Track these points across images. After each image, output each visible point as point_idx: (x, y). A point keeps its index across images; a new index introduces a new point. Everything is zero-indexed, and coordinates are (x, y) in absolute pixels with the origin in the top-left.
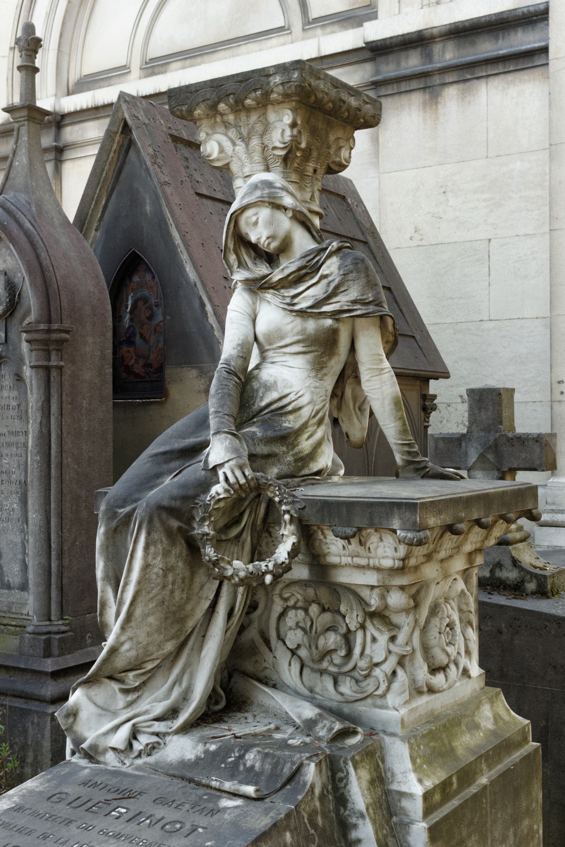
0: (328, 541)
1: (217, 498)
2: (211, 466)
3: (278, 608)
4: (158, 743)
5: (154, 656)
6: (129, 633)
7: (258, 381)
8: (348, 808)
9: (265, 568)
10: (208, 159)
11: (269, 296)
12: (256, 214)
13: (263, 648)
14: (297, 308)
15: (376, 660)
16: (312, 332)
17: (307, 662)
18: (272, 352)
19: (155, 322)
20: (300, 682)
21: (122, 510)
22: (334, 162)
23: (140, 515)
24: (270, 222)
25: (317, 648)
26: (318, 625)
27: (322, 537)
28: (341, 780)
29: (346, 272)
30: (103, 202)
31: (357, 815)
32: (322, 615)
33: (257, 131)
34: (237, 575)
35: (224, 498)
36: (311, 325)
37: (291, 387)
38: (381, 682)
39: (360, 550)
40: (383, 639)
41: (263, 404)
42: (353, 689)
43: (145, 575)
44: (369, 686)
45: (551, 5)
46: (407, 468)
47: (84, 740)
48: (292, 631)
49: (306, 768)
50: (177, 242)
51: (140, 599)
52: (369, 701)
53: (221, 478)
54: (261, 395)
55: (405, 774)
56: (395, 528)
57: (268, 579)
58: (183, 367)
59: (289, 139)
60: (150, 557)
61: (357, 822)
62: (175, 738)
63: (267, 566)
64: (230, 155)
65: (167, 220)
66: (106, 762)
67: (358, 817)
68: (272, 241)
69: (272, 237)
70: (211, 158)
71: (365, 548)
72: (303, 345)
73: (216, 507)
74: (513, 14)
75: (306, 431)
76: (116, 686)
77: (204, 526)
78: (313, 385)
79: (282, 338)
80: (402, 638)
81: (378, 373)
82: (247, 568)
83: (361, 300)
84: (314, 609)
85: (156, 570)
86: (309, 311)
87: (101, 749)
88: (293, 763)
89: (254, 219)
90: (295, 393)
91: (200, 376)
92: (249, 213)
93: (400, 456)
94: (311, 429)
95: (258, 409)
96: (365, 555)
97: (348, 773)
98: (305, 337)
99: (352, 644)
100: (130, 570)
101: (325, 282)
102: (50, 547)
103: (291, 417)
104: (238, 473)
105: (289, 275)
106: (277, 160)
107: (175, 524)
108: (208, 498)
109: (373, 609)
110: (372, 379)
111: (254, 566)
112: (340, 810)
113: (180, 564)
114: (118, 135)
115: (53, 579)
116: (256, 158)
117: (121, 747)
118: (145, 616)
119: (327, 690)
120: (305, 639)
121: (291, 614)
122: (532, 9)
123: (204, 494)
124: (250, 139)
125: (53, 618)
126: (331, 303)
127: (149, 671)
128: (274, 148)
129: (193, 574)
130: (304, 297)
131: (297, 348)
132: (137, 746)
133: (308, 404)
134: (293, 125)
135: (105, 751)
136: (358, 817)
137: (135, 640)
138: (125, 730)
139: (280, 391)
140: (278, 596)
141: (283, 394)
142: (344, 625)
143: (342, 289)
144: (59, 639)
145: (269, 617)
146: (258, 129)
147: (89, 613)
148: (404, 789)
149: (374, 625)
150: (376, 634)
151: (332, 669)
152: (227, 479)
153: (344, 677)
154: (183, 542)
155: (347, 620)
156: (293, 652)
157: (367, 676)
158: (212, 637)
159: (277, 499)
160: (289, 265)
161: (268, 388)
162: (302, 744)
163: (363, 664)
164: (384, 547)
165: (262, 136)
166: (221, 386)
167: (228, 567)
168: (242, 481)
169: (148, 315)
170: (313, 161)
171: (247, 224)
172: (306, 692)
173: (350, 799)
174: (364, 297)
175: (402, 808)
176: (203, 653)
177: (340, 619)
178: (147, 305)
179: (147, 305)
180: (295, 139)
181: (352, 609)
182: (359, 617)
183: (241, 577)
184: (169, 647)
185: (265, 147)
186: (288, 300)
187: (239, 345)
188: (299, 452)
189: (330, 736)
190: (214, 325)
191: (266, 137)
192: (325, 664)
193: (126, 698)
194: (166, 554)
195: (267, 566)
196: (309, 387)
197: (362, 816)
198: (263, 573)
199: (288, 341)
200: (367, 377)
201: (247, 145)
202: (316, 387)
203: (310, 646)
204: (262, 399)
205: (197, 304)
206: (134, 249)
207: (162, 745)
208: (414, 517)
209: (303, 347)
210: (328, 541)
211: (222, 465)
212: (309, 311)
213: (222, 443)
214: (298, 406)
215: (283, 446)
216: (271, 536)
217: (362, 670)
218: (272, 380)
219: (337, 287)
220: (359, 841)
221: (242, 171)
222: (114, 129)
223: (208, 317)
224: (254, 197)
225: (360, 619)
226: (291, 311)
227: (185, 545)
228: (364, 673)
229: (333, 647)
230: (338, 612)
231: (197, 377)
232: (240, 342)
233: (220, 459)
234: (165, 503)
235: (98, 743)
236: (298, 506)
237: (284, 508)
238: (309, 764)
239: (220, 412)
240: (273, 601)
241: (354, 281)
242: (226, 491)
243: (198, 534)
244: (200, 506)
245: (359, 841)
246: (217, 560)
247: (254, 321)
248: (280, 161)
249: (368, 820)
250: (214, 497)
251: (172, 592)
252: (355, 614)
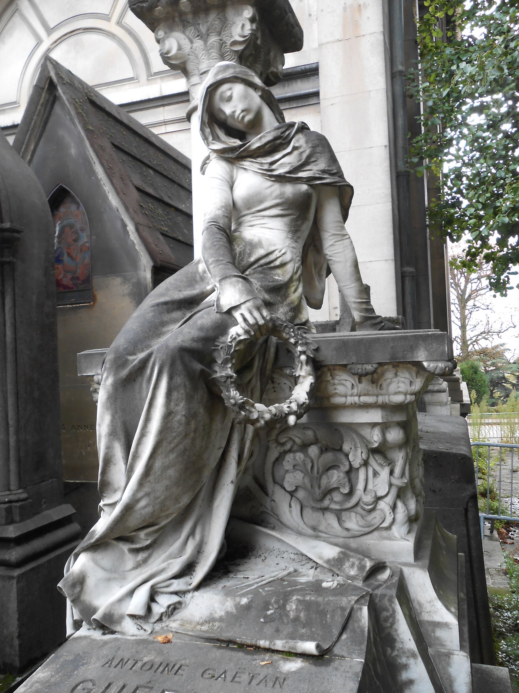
0: (336, 382)
1: (238, 339)
2: (225, 310)
3: (274, 454)
4: (180, 603)
5: (170, 511)
6: (146, 489)
7: (242, 240)
8: (396, 648)
9: (288, 409)
10: (166, 56)
11: (246, 164)
12: (230, 89)
13: (259, 493)
14: (276, 173)
15: (380, 493)
16: (290, 195)
17: (305, 503)
18: (250, 216)
19: (80, 243)
20: (303, 522)
21: (134, 357)
22: (272, 73)
23: (160, 360)
24: (245, 97)
25: (319, 487)
26: (320, 466)
27: (329, 378)
28: (386, 619)
29: (314, 145)
30: (32, 147)
31: (407, 655)
32: (323, 455)
33: (216, 28)
34: (263, 418)
35: (245, 339)
36: (289, 190)
37: (274, 245)
38: (388, 514)
39: (371, 388)
40: (384, 473)
41: (252, 259)
42: (360, 524)
43: (167, 424)
44: (375, 518)
45: (320, 64)
46: (365, 323)
47: (95, 610)
48: (291, 475)
49: (359, 613)
50: (99, 177)
51: (160, 451)
52: (376, 534)
53: (240, 319)
54: (249, 251)
55: (432, 603)
56: (420, 359)
57: (292, 420)
58: (109, 276)
59: (250, 32)
60: (172, 404)
61: (408, 662)
62: (196, 594)
63: (288, 407)
64: (187, 54)
65: (91, 159)
66: (123, 631)
67: (408, 657)
68: (247, 115)
69: (245, 111)
70: (169, 55)
71: (377, 386)
72: (281, 208)
73: (237, 349)
74: (295, 70)
75: (291, 285)
76: (125, 547)
77: (227, 368)
78: (291, 245)
79: (261, 202)
80: (398, 471)
81: (341, 239)
82: (270, 411)
83: (328, 170)
85: (178, 417)
86: (288, 175)
87: (116, 617)
88: (343, 609)
89: (228, 93)
90: (279, 251)
91: (124, 282)
93: (358, 313)
94: (295, 283)
95: (248, 264)
96: (376, 392)
97: (394, 611)
98: (283, 200)
99: (353, 480)
100: (148, 419)
101: (296, 153)
102: (7, 424)
103: (279, 271)
104: (256, 314)
105: (266, 144)
106: (233, 57)
107: (198, 366)
108: (229, 340)
109: (376, 445)
110: (335, 243)
111: (275, 407)
112: (386, 651)
113: (201, 410)
114: (45, 91)
115: (12, 453)
116: (214, 54)
117: (141, 612)
118: (165, 468)
119: (333, 527)
120: (307, 481)
121: (289, 457)
122: (307, 67)
123: (222, 336)
124: (208, 35)
125: (12, 488)
126: (305, 171)
127: (162, 528)
128: (235, 43)
129: (212, 420)
130: (281, 164)
132: (158, 609)
133: (291, 261)
134: (252, 20)
135: (121, 618)
136: (408, 657)
137: (152, 496)
138: (143, 593)
139: (266, 248)
140: (274, 441)
141: (270, 251)
142: (347, 463)
143: (313, 160)
144: (21, 507)
145: (264, 463)
146: (217, 26)
147: (43, 481)
148: (437, 618)
149: (376, 461)
150: (378, 468)
151: (334, 506)
152: (245, 320)
153: (348, 513)
154: (204, 386)
155: (351, 457)
156: (292, 494)
157: (370, 511)
158: (226, 485)
159: (292, 341)
160: (266, 135)
161: (253, 246)
162: (339, 586)
163: (368, 498)
164: (398, 383)
165: (219, 34)
166: (216, 239)
167: (253, 410)
168: (261, 322)
169: (74, 238)
170: (261, 64)
171: (222, 99)
172: (310, 532)
173: (398, 639)
174: (330, 168)
175: (438, 639)
176: (217, 503)
177: (343, 457)
178: (73, 230)
179: (73, 230)
180: (254, 32)
181: (356, 447)
182: (363, 455)
183: (266, 419)
184: (185, 500)
185: (223, 43)
186: (266, 167)
187: (222, 206)
188: (291, 303)
189: (364, 574)
190: (135, 241)
191: (225, 33)
192: (326, 502)
193: (136, 558)
194: (189, 398)
195: (288, 407)
196: (288, 246)
197: (414, 656)
198: (286, 414)
200: (331, 243)
201: (206, 42)
202: (293, 248)
203: (312, 486)
204: (250, 255)
205: (119, 225)
206: (61, 184)
207: (183, 605)
208: (442, 348)
209: (281, 210)
210: (336, 382)
211: (236, 308)
212: (288, 175)
213: (235, 286)
214: (284, 262)
215: (278, 296)
216: (273, 382)
217: (368, 505)
218: (256, 240)
219: (309, 157)
220: (411, 682)
221: (198, 69)
222: (42, 85)
223: (129, 235)
224: (227, 74)
225: (364, 456)
226: (270, 176)
227: (206, 390)
228: (370, 507)
229: (335, 486)
230: (341, 450)
231: (121, 284)
232: (223, 204)
233: (236, 301)
234: (187, 344)
235: (112, 612)
236: (312, 347)
237: (299, 348)
238: (361, 609)
239: (222, 260)
240: (268, 448)
241: (321, 153)
242: (247, 332)
243: (222, 377)
244: (221, 348)
245: (411, 682)
246: (243, 403)
247: (231, 188)
248: (236, 57)
249: (420, 659)
250: (235, 338)
251: (194, 440)
252: (359, 451)
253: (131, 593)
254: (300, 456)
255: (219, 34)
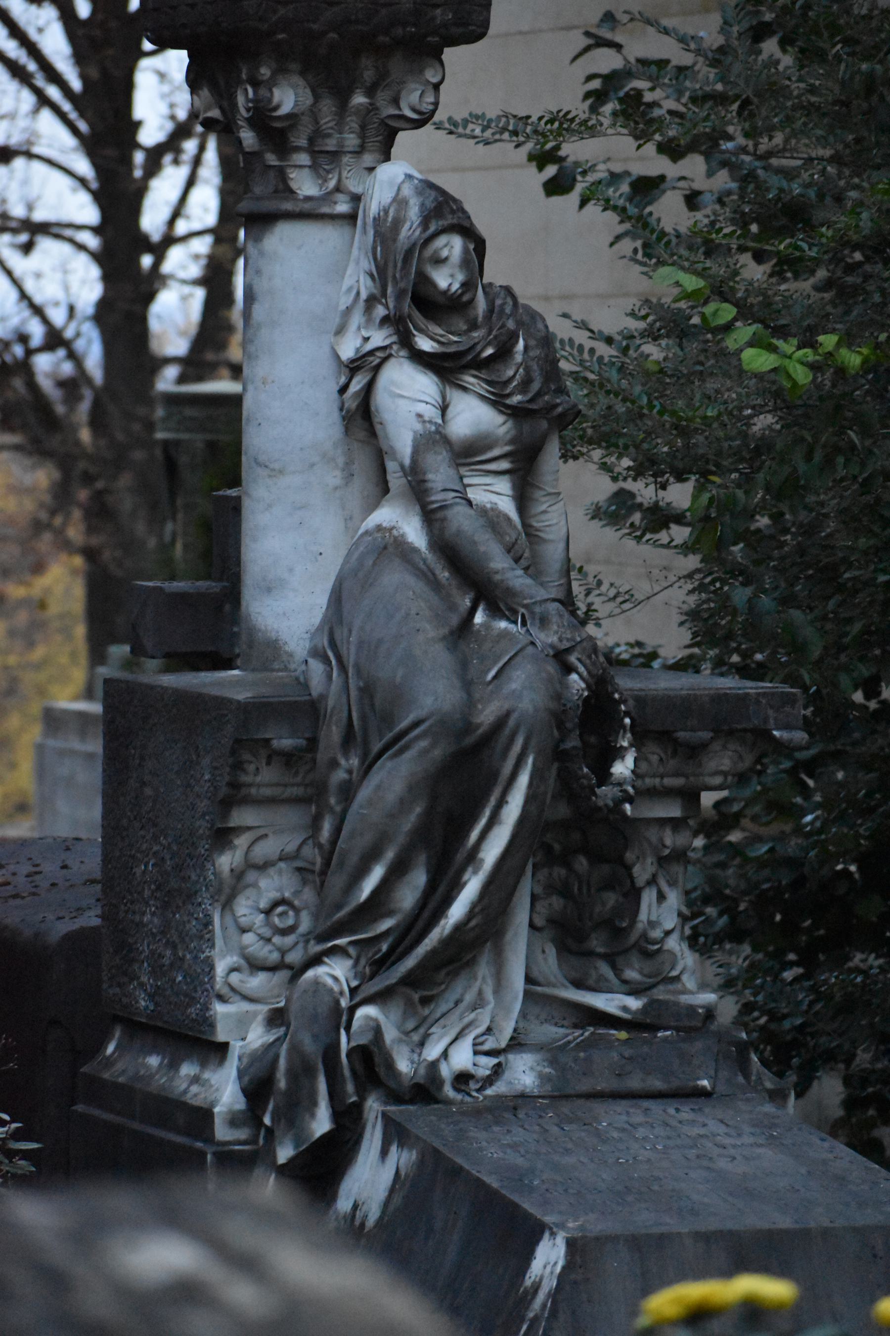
4: (499, 1065)
10: (268, 114)
11: (469, 379)
42: (646, 971)
79: (490, 447)
84: (582, 863)
92: (441, 241)
110: (549, 509)
131: (505, 465)
150: (665, 888)
155: (636, 870)
199: (496, 452)
253: (445, 1054)
254: (560, 872)
255: (370, 92)
